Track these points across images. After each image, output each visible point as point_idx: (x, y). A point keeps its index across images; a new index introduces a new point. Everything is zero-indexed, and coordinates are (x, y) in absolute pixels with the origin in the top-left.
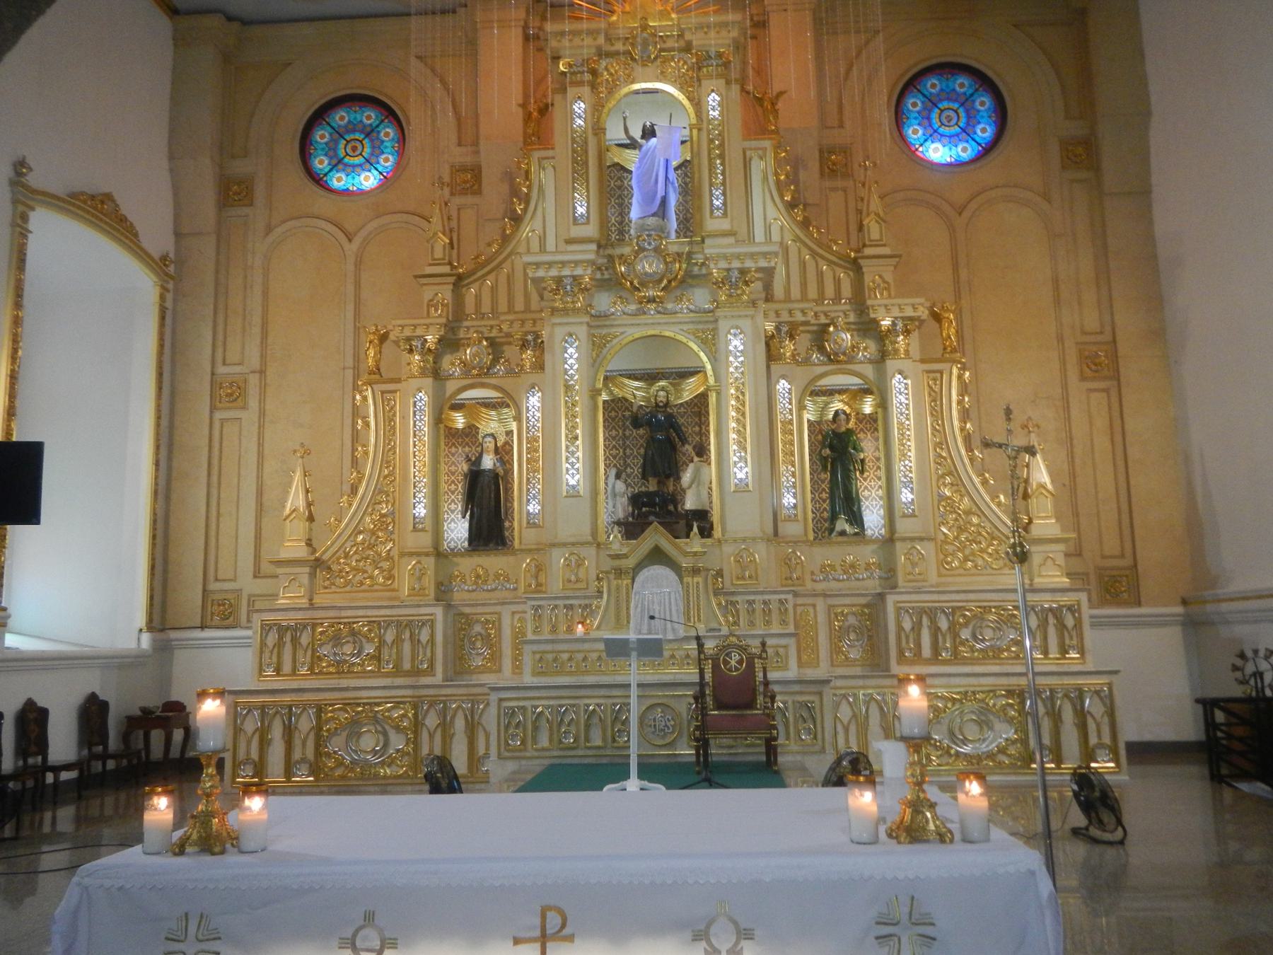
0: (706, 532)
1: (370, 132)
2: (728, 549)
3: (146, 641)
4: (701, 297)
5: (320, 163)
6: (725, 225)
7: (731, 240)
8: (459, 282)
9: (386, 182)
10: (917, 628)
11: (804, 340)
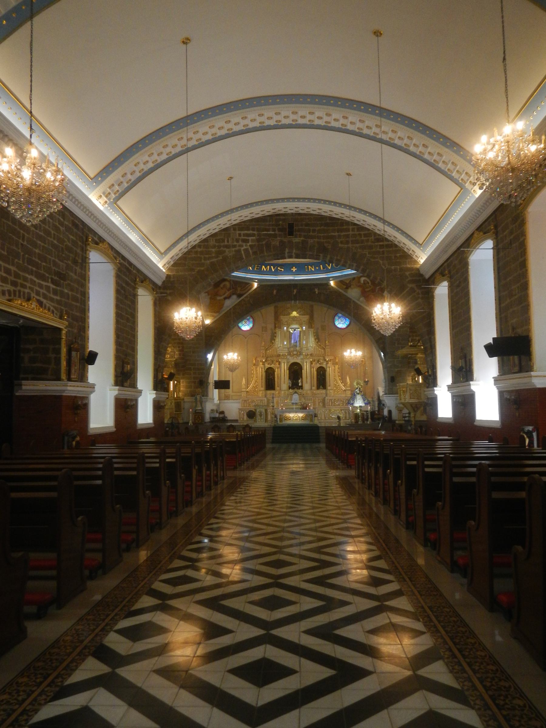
0: (302, 389)
1: (248, 320)
2: (305, 391)
3: (218, 402)
4: (302, 357)
5: (240, 325)
6: (305, 346)
7: (306, 349)
8: (266, 350)
9: (251, 329)
10: (329, 401)
11: (316, 361)
